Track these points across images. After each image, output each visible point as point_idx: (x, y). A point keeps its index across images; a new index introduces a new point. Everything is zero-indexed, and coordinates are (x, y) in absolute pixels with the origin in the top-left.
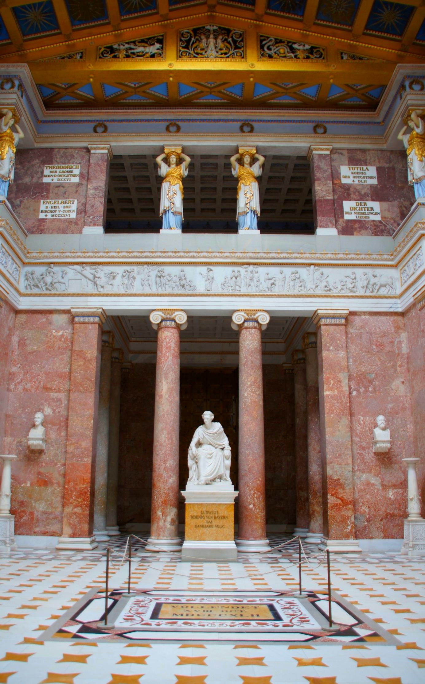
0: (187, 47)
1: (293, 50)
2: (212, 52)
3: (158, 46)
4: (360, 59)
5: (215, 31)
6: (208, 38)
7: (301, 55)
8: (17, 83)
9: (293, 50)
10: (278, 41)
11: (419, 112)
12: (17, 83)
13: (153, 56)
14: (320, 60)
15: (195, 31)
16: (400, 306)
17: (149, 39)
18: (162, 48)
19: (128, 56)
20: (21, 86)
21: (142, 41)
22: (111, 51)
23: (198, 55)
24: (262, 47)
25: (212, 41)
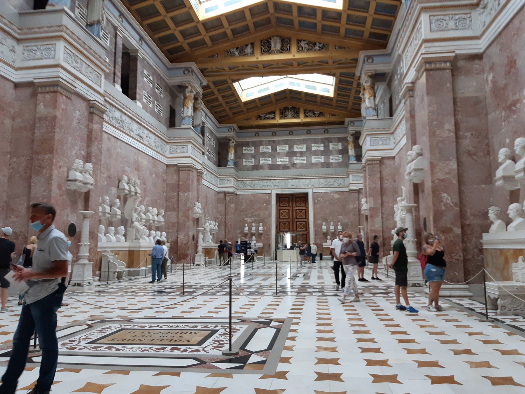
0: (282, 115)
1: (314, 114)
2: (290, 115)
3: (273, 114)
4: (335, 115)
5: (291, 108)
6: (288, 111)
7: (317, 115)
8: (232, 128)
9: (314, 114)
10: (310, 111)
11: (352, 133)
12: (232, 128)
13: (272, 118)
14: (322, 117)
15: (284, 108)
16: (347, 189)
17: (271, 112)
18: (275, 116)
19: (265, 119)
20: (234, 129)
21: (269, 113)
22: (259, 117)
23: (286, 117)
24: (305, 113)
25: (290, 112)
